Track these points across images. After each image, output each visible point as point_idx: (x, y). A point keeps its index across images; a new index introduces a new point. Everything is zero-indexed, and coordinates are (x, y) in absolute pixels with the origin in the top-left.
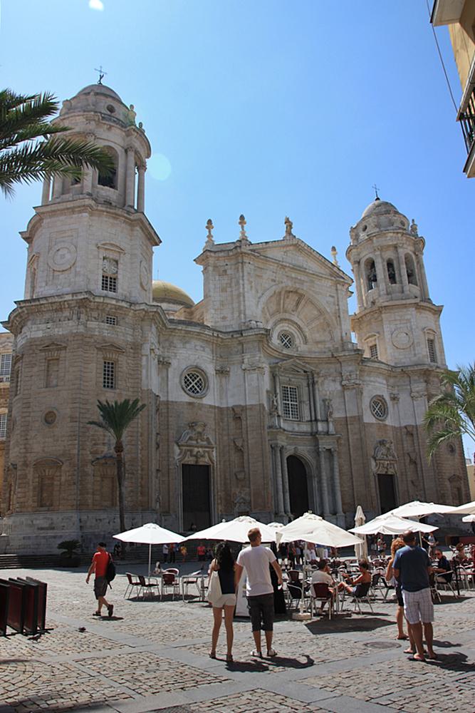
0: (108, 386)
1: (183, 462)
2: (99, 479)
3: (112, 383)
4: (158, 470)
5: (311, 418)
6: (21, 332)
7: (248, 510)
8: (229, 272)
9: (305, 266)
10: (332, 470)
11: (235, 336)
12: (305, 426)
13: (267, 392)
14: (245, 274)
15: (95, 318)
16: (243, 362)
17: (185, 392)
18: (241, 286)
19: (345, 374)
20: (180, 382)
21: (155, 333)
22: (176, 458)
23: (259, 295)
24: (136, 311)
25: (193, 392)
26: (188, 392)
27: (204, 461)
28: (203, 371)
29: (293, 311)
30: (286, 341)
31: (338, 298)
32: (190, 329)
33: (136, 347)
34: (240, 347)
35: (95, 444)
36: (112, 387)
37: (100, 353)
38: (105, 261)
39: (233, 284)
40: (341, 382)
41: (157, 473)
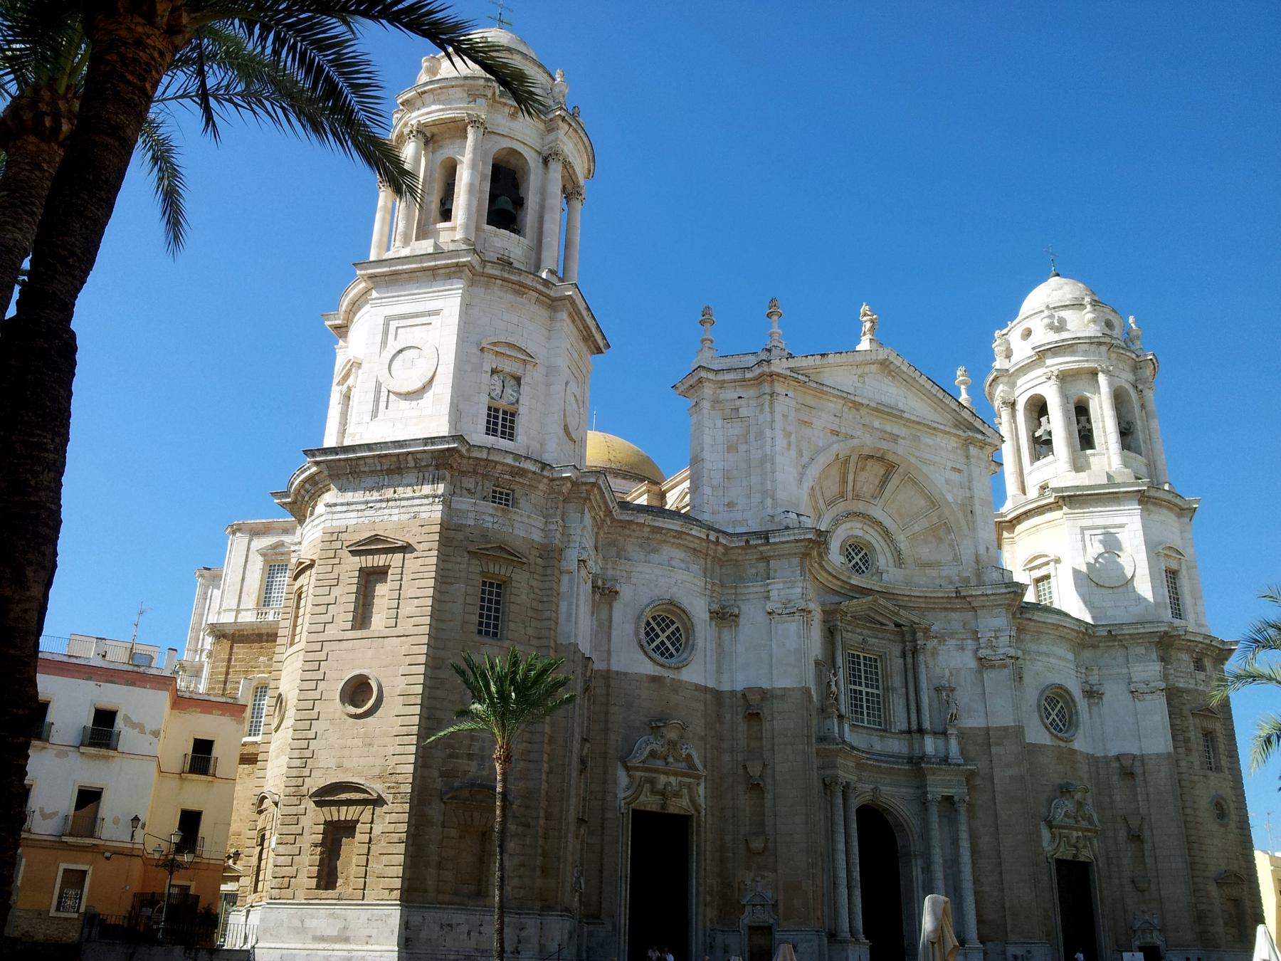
0: (487, 633)
1: (633, 806)
2: (453, 833)
3: (496, 626)
4: (581, 821)
5: (909, 723)
6: (312, 514)
7: (771, 921)
8: (744, 412)
9: (901, 406)
10: (955, 842)
11: (751, 542)
12: (896, 742)
13: (817, 663)
14: (778, 417)
15: (468, 490)
16: (768, 598)
17: (645, 652)
18: (769, 440)
19: (985, 635)
20: (637, 633)
21: (590, 529)
22: (621, 795)
23: (805, 459)
24: (553, 480)
25: (662, 654)
26: (652, 654)
27: (679, 805)
28: (684, 611)
29: (873, 497)
30: (857, 559)
31: (970, 475)
32: (661, 525)
33: (550, 555)
34: (762, 566)
35: (451, 756)
36: (495, 634)
37: (474, 561)
38: (495, 377)
39: (752, 438)
40: (977, 650)
41: (579, 828)
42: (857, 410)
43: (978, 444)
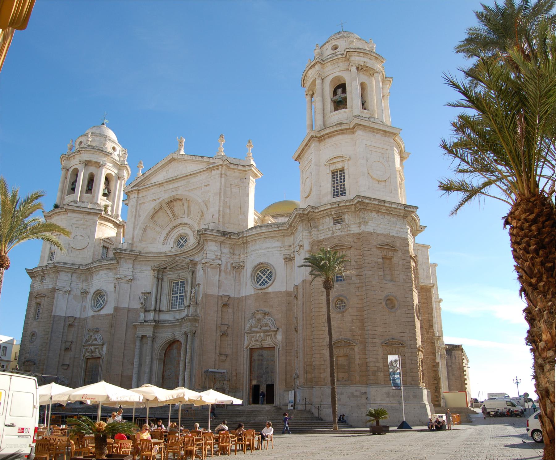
42: (162, 186)
43: (214, 168)
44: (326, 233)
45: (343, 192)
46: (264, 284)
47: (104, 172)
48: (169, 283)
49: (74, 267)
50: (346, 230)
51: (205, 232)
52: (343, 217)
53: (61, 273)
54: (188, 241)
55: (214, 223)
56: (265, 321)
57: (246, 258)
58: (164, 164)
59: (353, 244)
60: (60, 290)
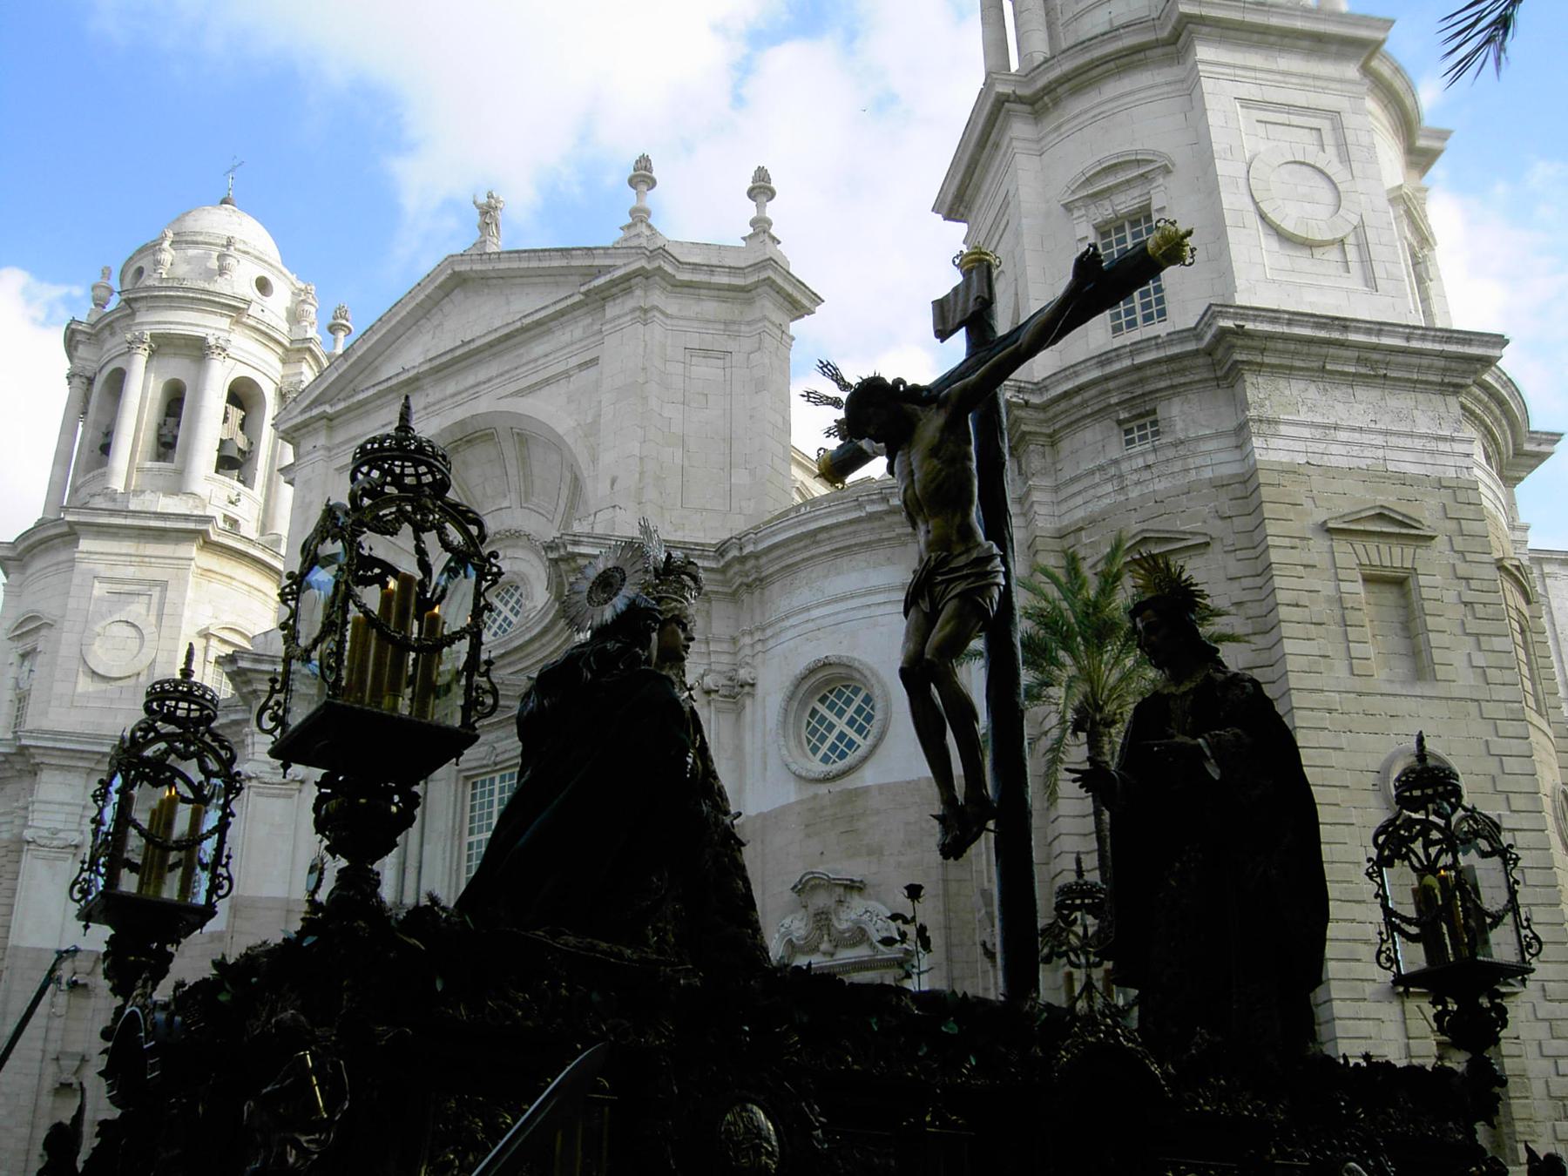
43: (614, 290)
44: (1092, 492)
45: (1154, 309)
46: (842, 755)
47: (218, 379)
48: (453, 787)
49: (96, 748)
50: (1178, 466)
51: (577, 550)
52: (1159, 416)
53: (45, 776)
54: (528, 604)
55: (614, 507)
56: (844, 922)
57: (759, 647)
58: (423, 301)
59: (1216, 528)
60: (38, 841)
